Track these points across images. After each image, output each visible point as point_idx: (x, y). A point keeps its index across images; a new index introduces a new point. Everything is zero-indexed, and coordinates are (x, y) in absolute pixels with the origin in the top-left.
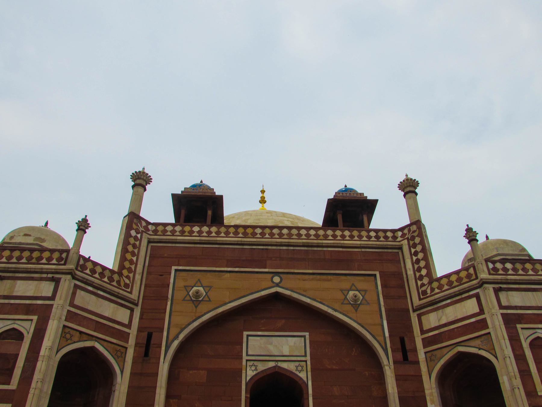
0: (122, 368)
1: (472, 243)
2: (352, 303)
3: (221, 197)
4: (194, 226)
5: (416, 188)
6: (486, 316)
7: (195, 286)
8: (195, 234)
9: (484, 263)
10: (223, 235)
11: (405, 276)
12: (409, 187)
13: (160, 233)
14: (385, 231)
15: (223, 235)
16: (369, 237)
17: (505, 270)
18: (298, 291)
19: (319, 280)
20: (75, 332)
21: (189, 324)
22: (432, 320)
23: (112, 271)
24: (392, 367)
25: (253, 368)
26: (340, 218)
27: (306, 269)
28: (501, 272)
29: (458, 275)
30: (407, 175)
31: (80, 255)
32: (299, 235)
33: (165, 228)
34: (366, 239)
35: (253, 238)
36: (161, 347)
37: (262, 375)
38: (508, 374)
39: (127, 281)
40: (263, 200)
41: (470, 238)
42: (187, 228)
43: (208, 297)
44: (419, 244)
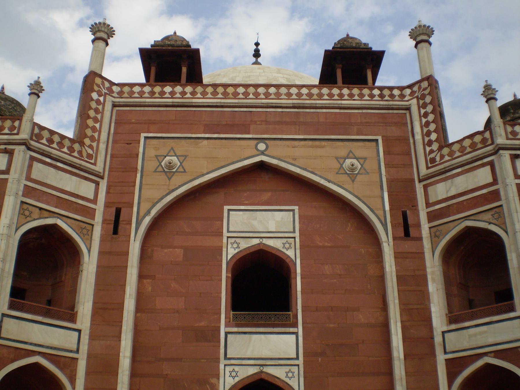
0: (89, 247)
1: (490, 102)
2: (348, 172)
3: (197, 51)
4: (166, 86)
5: (430, 37)
7: (167, 155)
8: (167, 95)
9: (502, 125)
10: (199, 95)
12: (422, 36)
13: (126, 95)
14: (391, 89)
15: (199, 95)
16: (372, 96)
19: (312, 147)
20: (34, 208)
21: (162, 199)
24: (391, 244)
25: (235, 245)
27: (296, 134)
31: (34, 123)
32: (289, 95)
34: (369, 98)
35: (235, 98)
36: (131, 224)
39: (90, 151)
41: (489, 97)
42: (157, 89)
43: (183, 167)
44: (429, 104)
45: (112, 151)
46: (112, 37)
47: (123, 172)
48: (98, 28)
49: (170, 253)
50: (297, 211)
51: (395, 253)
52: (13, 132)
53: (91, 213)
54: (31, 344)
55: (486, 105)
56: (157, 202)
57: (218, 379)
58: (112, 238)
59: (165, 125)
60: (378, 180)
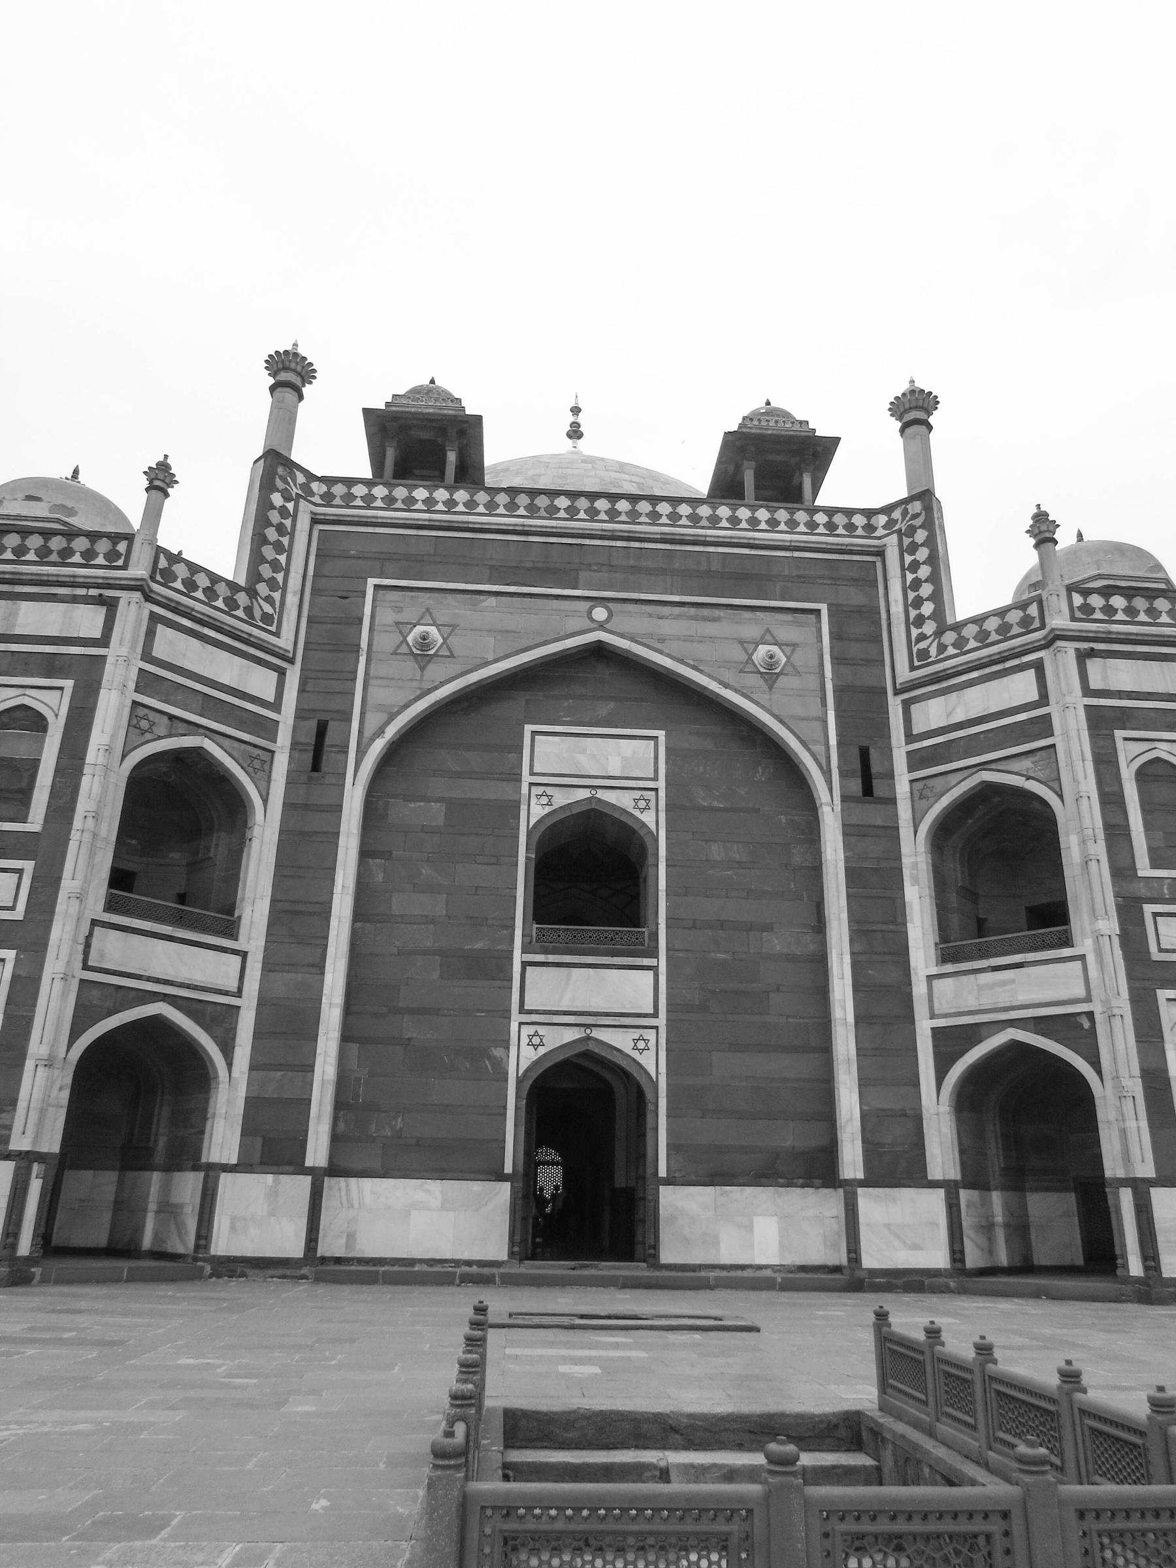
0: (264, 794)
2: (762, 670)
3: (478, 419)
5: (930, 414)
6: (1052, 709)
9: (1063, 593)
11: (884, 616)
12: (914, 411)
14: (849, 512)
15: (481, 509)
16: (812, 525)
17: (1109, 610)
18: (643, 641)
19: (695, 618)
20: (158, 715)
21: (407, 706)
22: (934, 713)
23: (233, 586)
24: (838, 808)
25: (544, 800)
26: (749, 478)
28: (1098, 615)
29: (1003, 619)
30: (912, 382)
32: (654, 516)
33: (349, 489)
35: (551, 519)
36: (346, 753)
37: (562, 816)
38: (1081, 831)
39: (268, 609)
40: (575, 432)
41: (1042, 536)
42: (400, 492)
43: (448, 647)
44: (922, 545)
46: (311, 383)
47: (330, 651)
48: (283, 362)
49: (421, 812)
51: (844, 825)
53: (269, 729)
54: (149, 979)
55: (1035, 553)
56: (399, 713)
57: (508, 1049)
58: (310, 779)
60: (817, 686)
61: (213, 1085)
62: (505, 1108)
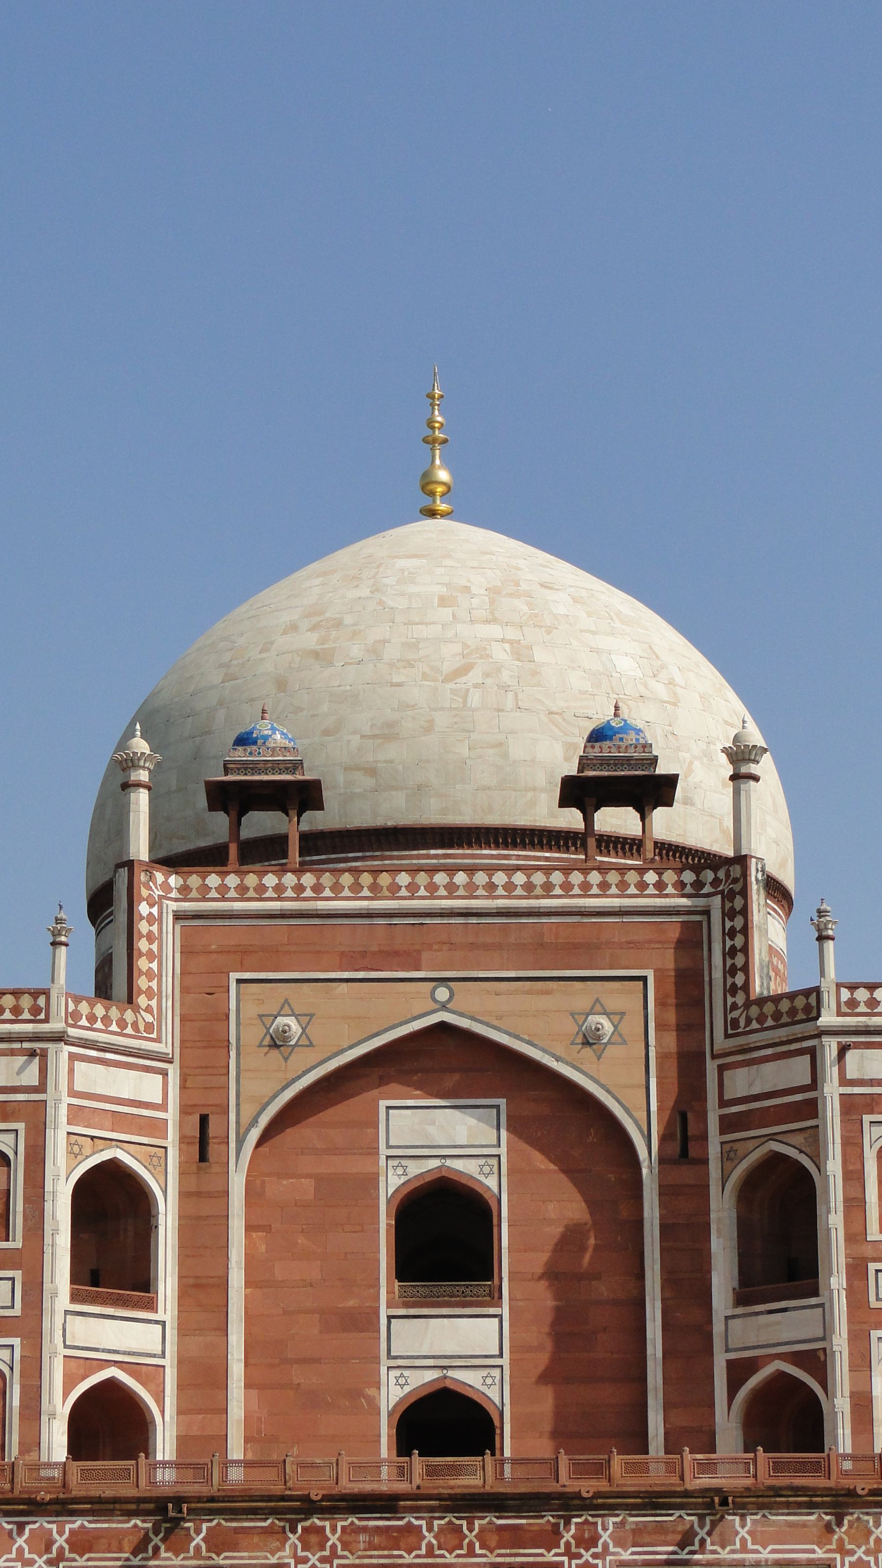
7: (279, 1015)
8: (270, 894)
11: (707, 979)
15: (327, 893)
19: (529, 992)
21: (275, 1097)
22: (741, 1083)
24: (656, 1171)
25: (400, 1171)
33: (204, 880)
37: (417, 1184)
39: (149, 1018)
45: (181, 1009)
47: (205, 1047)
50: (503, 1108)
52: (38, 1018)
54: (104, 1351)
56: (268, 1104)
58: (199, 1169)
59: (271, 956)
61: (151, 1428)
62: (379, 1436)
